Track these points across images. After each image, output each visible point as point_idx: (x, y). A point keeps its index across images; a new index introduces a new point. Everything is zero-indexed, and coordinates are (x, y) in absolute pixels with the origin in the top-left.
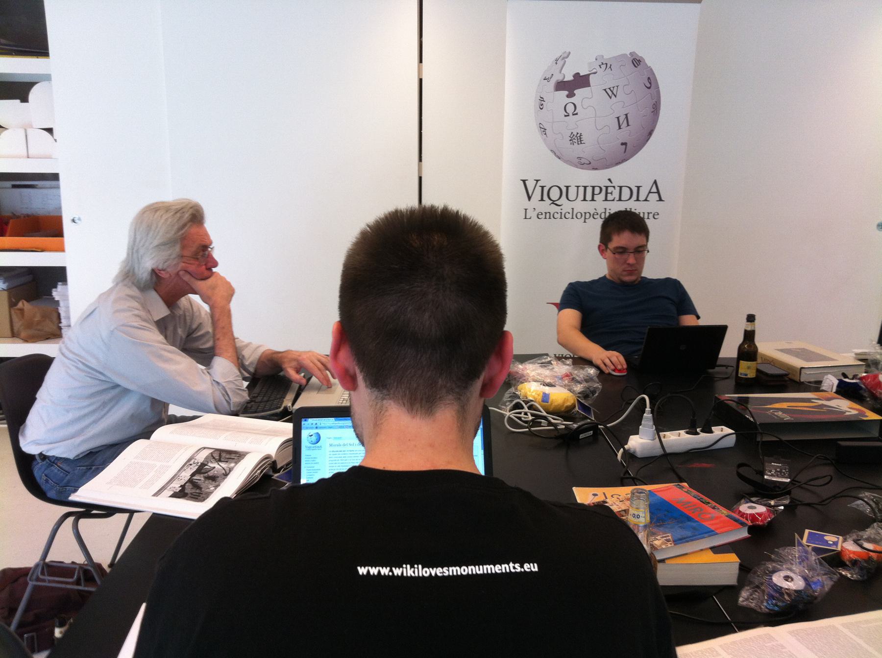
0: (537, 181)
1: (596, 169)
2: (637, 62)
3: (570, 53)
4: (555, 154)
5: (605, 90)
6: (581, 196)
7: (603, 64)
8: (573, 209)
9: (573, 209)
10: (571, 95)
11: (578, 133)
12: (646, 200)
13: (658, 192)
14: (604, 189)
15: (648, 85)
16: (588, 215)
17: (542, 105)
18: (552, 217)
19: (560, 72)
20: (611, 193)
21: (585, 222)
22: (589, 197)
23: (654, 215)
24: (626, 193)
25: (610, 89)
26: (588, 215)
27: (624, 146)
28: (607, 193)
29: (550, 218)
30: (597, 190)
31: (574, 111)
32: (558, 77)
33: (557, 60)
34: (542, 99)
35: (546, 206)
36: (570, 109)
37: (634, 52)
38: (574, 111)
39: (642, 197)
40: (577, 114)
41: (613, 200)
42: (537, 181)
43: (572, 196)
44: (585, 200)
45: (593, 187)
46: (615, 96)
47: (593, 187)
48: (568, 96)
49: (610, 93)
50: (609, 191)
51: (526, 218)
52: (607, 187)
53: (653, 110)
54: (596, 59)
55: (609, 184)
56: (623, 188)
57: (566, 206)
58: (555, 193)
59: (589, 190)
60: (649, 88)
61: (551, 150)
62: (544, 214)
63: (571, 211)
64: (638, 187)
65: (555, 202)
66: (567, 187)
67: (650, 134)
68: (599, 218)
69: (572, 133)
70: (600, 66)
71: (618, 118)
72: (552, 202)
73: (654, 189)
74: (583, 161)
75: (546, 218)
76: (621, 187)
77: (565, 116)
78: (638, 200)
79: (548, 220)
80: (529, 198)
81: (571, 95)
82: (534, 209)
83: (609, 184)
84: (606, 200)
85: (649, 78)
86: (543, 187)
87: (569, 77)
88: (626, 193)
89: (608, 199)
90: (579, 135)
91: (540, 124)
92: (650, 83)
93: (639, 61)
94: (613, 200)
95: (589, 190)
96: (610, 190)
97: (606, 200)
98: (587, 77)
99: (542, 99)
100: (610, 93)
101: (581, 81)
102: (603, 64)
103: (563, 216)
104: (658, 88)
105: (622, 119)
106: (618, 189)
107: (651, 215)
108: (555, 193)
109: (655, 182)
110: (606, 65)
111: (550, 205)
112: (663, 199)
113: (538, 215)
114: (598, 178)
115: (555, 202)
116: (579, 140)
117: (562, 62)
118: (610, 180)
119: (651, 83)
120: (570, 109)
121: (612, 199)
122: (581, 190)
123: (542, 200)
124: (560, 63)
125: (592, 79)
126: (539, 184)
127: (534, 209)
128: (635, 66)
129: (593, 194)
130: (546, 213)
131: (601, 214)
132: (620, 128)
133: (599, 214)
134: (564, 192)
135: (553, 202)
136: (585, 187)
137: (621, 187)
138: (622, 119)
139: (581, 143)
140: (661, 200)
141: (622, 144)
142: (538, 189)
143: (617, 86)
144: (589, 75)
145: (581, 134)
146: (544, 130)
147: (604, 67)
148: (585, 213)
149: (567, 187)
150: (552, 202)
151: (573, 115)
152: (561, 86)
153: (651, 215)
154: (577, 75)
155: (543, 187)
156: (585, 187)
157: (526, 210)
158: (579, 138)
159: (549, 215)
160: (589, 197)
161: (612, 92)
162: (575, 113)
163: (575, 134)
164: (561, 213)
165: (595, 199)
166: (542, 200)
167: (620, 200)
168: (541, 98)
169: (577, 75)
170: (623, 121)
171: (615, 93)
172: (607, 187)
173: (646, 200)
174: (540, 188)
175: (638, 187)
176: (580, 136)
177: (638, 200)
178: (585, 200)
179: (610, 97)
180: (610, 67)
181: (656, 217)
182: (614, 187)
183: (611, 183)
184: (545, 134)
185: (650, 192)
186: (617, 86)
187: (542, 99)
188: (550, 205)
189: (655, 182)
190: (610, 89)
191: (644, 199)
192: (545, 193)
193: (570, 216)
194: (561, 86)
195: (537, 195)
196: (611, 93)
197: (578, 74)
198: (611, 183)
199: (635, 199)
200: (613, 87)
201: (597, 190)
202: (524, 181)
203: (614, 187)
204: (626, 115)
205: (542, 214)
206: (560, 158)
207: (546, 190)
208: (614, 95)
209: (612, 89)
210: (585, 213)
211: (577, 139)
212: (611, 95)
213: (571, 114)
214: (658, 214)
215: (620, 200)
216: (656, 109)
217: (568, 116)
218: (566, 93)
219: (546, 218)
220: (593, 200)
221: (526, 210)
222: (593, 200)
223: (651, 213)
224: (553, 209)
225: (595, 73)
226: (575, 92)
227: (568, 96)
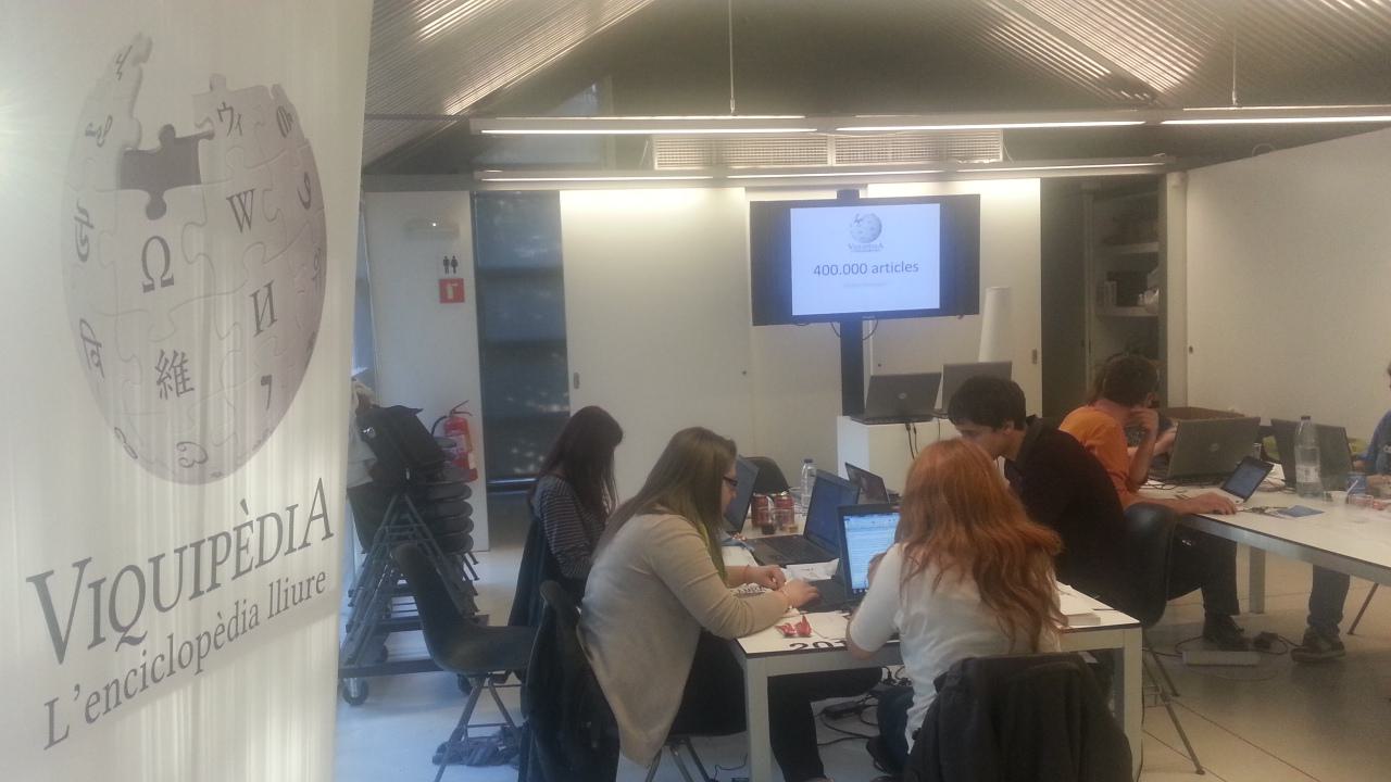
5: (230, 199)
10: (156, 210)
11: (176, 354)
17: (85, 241)
31: (163, 275)
38: (163, 275)
43: (168, 595)
54: (211, 87)
72: (120, 635)
81: (156, 210)
86: (96, 586)
87: (151, 143)
90: (178, 362)
91: (82, 321)
98: (191, 143)
116: (180, 379)
126: (90, 575)
139: (185, 391)
142: (87, 596)
143: (252, 191)
144: (196, 138)
145: (183, 354)
155: (96, 586)
157: (51, 704)
158: (178, 369)
163: (169, 356)
168: (83, 211)
176: (181, 365)
184: (98, 364)
186: (252, 191)
187: (84, 218)
202: (40, 581)
213: (158, 284)
221: (51, 704)
225: (210, 136)
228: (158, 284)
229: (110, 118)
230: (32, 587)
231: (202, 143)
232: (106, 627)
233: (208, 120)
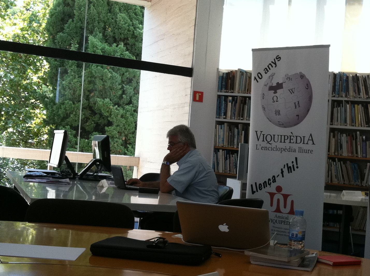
0: (261, 132)
1: (286, 127)
2: (302, 76)
3: (275, 73)
4: (269, 119)
5: (289, 90)
6: (279, 141)
7: (288, 78)
8: (276, 146)
9: (276, 146)
10: (275, 92)
11: (278, 110)
12: (307, 143)
13: (312, 140)
14: (289, 137)
15: (307, 87)
16: (289, 151)
17: (264, 97)
18: (267, 149)
19: (271, 82)
20: (292, 139)
21: (281, 153)
22: (283, 141)
23: (311, 151)
24: (299, 139)
25: (291, 89)
26: (289, 151)
27: (298, 117)
28: (290, 139)
29: (267, 150)
30: (286, 138)
31: (277, 100)
32: (271, 85)
33: (269, 77)
34: (264, 94)
35: (265, 144)
36: (275, 99)
37: (301, 72)
38: (277, 100)
39: (306, 142)
40: (278, 101)
41: (293, 143)
42: (261, 132)
43: (276, 140)
44: (281, 142)
45: (285, 136)
46: (294, 93)
47: (285, 136)
48: (274, 93)
49: (291, 92)
50: (292, 138)
51: (257, 149)
52: (290, 136)
53: (309, 99)
55: (291, 135)
56: (298, 137)
57: (274, 144)
58: (269, 138)
59: (283, 137)
60: (307, 89)
61: (267, 118)
62: (264, 148)
63: (275, 147)
64: (304, 137)
65: (269, 142)
66: (274, 135)
67: (308, 111)
68: (287, 151)
69: (276, 110)
70: (287, 79)
71: (295, 103)
72: (267, 142)
73: (310, 138)
74: (280, 123)
75: (265, 150)
76: (297, 137)
77: (273, 102)
78: (304, 143)
79: (264, 151)
80: (258, 140)
82: (260, 145)
83: (291, 135)
84: (290, 142)
85: (307, 84)
86: (264, 135)
87: (275, 84)
88: (299, 139)
89: (291, 142)
90: (278, 111)
91: (263, 105)
92: (308, 87)
93: (303, 76)
94: (293, 143)
95: (283, 137)
96: (292, 137)
97: (290, 142)
99: (264, 94)
100: (291, 92)
101: (279, 86)
102: (288, 78)
103: (272, 149)
104: (311, 88)
105: (297, 104)
106: (295, 137)
107: (309, 152)
108: (269, 138)
109: (311, 135)
110: (289, 78)
111: (267, 143)
112: (315, 143)
113: (262, 148)
114: (286, 131)
115: (269, 142)
117: (272, 77)
118: (292, 133)
119: (308, 86)
120: (275, 99)
121: (293, 142)
122: (280, 137)
123: (263, 141)
124: (271, 78)
125: (284, 85)
126: (262, 133)
127: (260, 145)
128: (302, 79)
129: (285, 139)
130: (265, 147)
131: (288, 149)
132: (296, 108)
133: (287, 149)
134: (273, 137)
135: (268, 142)
136: (281, 136)
137: (297, 137)
138: (297, 104)
140: (313, 144)
141: (297, 116)
142: (262, 136)
143: (294, 88)
144: (282, 83)
146: (264, 109)
147: (289, 79)
148: (281, 148)
149: (274, 135)
150: (267, 142)
151: (276, 101)
152: (271, 88)
153: (309, 152)
154: (278, 83)
155: (264, 135)
156: (281, 136)
157: (257, 145)
159: (266, 149)
160: (283, 141)
161: (292, 91)
162: (277, 101)
163: (277, 110)
164: (271, 148)
165: (285, 142)
166: (263, 141)
167: (296, 143)
168: (264, 94)
169: (278, 83)
170: (297, 105)
171: (293, 91)
172: (290, 136)
173: (307, 143)
174: (263, 135)
175: (304, 137)
176: (279, 112)
177: (304, 143)
178: (281, 142)
179: (291, 94)
180: (291, 79)
181: (312, 152)
182: (294, 136)
183: (293, 134)
184: (265, 110)
185: (309, 140)
186: (294, 88)
188: (267, 143)
189: (311, 135)
190: (291, 89)
191: (306, 143)
192: (265, 138)
193: (275, 149)
194: (271, 88)
195: (261, 139)
196: (292, 91)
197: (278, 83)
198: (293, 134)
199: (303, 143)
200: (293, 89)
201: (286, 138)
202: (256, 132)
203: (294, 136)
204: (298, 102)
205: (263, 148)
206: (271, 122)
207: (265, 136)
208: (293, 92)
209: (292, 90)
210: (281, 148)
211: (278, 113)
212: (291, 92)
213: (275, 101)
214: (313, 151)
215: (296, 143)
216: (310, 99)
217: (274, 102)
218: (273, 91)
219: (265, 150)
220: (284, 142)
221: (257, 145)
222: (284, 142)
223: (309, 150)
224: (268, 145)
225: (285, 82)
226: (277, 91)
227: (274, 93)
228: (275, 101)
229: (268, 83)
230: (255, 132)
231: (283, 84)
232: (265, 140)
233: (285, 80)
